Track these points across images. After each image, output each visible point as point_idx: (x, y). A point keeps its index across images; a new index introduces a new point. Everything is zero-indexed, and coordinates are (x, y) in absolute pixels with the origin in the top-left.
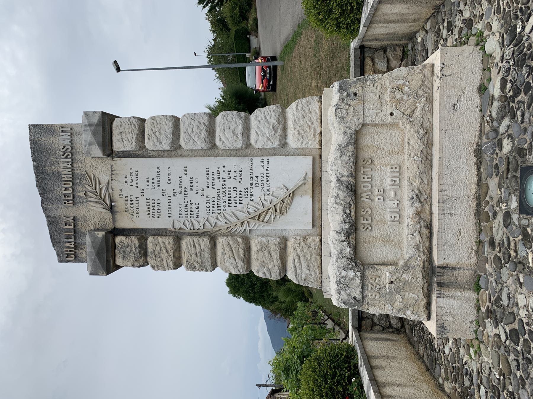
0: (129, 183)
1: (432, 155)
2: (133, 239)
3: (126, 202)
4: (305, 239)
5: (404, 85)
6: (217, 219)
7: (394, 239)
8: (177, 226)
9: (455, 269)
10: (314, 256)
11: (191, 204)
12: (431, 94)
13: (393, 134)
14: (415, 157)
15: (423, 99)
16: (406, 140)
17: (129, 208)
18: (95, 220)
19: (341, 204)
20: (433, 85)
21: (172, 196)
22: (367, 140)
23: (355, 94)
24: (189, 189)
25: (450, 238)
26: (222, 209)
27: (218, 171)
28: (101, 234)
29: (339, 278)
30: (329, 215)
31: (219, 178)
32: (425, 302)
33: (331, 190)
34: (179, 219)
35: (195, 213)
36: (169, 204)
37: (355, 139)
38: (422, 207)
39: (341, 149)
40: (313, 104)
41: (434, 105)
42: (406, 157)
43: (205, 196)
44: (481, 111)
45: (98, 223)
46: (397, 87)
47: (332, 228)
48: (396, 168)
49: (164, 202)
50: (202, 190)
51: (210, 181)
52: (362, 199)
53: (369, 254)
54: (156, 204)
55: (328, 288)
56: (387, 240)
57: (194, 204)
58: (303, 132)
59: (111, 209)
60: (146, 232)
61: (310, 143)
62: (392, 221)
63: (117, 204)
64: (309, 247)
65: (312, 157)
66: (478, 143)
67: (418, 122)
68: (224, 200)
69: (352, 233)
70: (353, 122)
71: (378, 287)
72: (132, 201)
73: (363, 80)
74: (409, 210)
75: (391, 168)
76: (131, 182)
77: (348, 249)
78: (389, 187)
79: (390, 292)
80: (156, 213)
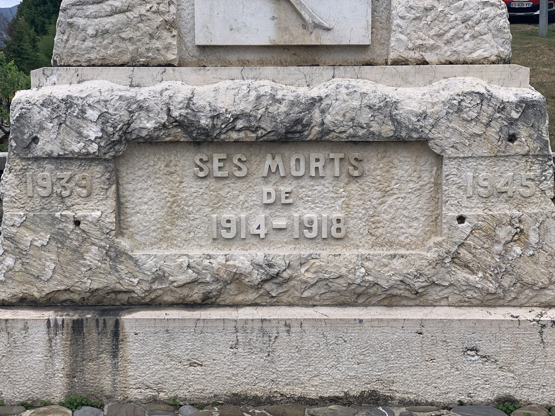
1: (366, 306)
4: (170, 25)
5: (527, 245)
7: (177, 223)
9: (115, 355)
10: (131, 48)
12: (501, 302)
13: (415, 224)
14: (363, 270)
15: (491, 287)
16: (403, 251)
19: (256, 108)
20: (521, 306)
22: (405, 170)
23: (512, 138)
25: (183, 346)
29: (80, 102)
30: (229, 83)
32: (37, 295)
33: (289, 87)
37: (409, 140)
38: (252, 287)
39: (387, 109)
40: (493, 43)
41: (476, 309)
42: (362, 251)
44: (461, 403)
46: (522, 231)
47: (199, 89)
48: (339, 230)
52: (269, 157)
53: (140, 173)
55: (54, 78)
56: (175, 212)
58: (429, 19)
61: (403, 37)
62: (219, 224)
64: (151, 36)
65: (367, 42)
66: (392, 398)
67: (440, 275)
69: (190, 134)
70: (448, 135)
71: (65, 193)
73: (544, 156)
74: (243, 258)
75: (338, 221)
77: (150, 125)
78: (296, 215)
79: (54, 218)
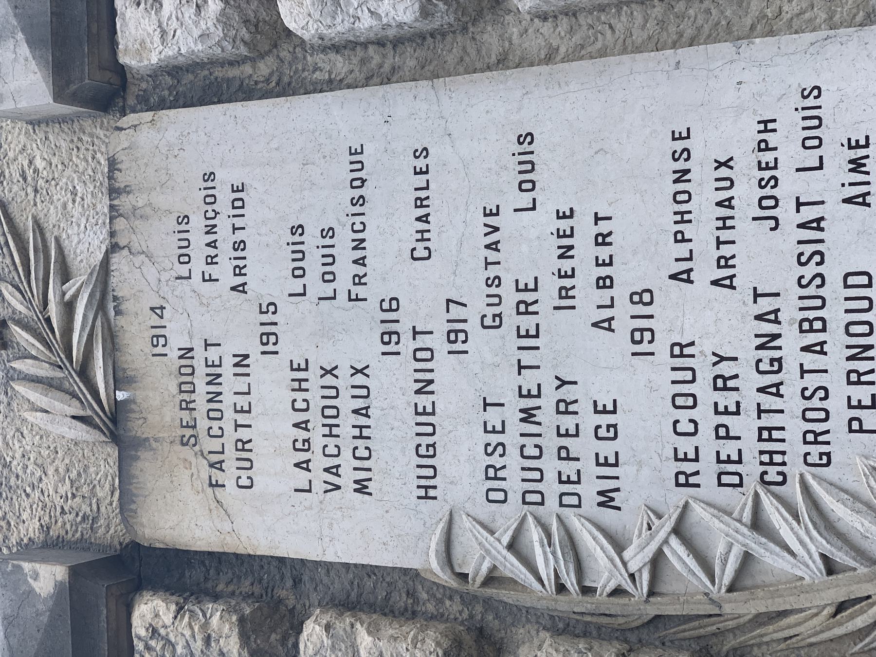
0: (198, 266)
2: (215, 621)
3: (187, 388)
6: (758, 524)
8: (479, 554)
11: (565, 408)
17: (203, 424)
18: (48, 485)
21: (438, 342)
24: (550, 287)
26: (794, 447)
27: (764, 147)
28: (47, 577)
31: (768, 204)
34: (485, 511)
35: (590, 469)
36: (424, 401)
43: (661, 347)
45: (59, 502)
49: (392, 380)
50: (642, 297)
51: (703, 233)
54: (346, 404)
57: (584, 408)
59: (114, 423)
60: (297, 582)
63: (140, 395)
68: (812, 381)
72: (214, 379)
76: (211, 261)
80: (346, 461)
